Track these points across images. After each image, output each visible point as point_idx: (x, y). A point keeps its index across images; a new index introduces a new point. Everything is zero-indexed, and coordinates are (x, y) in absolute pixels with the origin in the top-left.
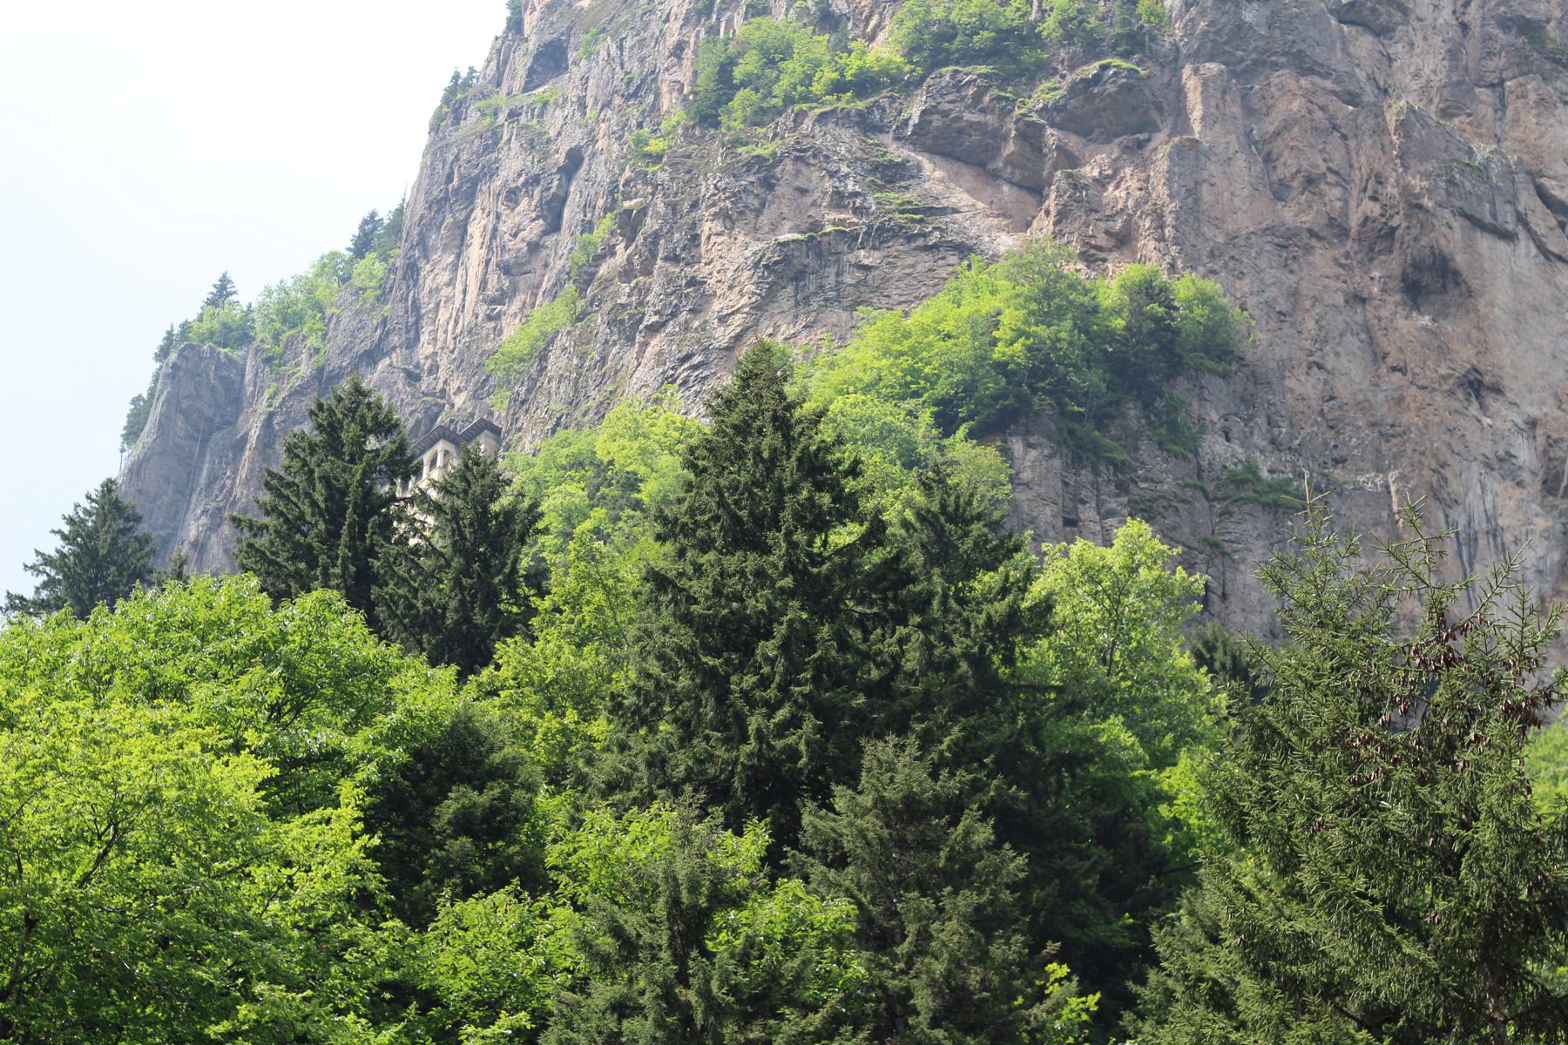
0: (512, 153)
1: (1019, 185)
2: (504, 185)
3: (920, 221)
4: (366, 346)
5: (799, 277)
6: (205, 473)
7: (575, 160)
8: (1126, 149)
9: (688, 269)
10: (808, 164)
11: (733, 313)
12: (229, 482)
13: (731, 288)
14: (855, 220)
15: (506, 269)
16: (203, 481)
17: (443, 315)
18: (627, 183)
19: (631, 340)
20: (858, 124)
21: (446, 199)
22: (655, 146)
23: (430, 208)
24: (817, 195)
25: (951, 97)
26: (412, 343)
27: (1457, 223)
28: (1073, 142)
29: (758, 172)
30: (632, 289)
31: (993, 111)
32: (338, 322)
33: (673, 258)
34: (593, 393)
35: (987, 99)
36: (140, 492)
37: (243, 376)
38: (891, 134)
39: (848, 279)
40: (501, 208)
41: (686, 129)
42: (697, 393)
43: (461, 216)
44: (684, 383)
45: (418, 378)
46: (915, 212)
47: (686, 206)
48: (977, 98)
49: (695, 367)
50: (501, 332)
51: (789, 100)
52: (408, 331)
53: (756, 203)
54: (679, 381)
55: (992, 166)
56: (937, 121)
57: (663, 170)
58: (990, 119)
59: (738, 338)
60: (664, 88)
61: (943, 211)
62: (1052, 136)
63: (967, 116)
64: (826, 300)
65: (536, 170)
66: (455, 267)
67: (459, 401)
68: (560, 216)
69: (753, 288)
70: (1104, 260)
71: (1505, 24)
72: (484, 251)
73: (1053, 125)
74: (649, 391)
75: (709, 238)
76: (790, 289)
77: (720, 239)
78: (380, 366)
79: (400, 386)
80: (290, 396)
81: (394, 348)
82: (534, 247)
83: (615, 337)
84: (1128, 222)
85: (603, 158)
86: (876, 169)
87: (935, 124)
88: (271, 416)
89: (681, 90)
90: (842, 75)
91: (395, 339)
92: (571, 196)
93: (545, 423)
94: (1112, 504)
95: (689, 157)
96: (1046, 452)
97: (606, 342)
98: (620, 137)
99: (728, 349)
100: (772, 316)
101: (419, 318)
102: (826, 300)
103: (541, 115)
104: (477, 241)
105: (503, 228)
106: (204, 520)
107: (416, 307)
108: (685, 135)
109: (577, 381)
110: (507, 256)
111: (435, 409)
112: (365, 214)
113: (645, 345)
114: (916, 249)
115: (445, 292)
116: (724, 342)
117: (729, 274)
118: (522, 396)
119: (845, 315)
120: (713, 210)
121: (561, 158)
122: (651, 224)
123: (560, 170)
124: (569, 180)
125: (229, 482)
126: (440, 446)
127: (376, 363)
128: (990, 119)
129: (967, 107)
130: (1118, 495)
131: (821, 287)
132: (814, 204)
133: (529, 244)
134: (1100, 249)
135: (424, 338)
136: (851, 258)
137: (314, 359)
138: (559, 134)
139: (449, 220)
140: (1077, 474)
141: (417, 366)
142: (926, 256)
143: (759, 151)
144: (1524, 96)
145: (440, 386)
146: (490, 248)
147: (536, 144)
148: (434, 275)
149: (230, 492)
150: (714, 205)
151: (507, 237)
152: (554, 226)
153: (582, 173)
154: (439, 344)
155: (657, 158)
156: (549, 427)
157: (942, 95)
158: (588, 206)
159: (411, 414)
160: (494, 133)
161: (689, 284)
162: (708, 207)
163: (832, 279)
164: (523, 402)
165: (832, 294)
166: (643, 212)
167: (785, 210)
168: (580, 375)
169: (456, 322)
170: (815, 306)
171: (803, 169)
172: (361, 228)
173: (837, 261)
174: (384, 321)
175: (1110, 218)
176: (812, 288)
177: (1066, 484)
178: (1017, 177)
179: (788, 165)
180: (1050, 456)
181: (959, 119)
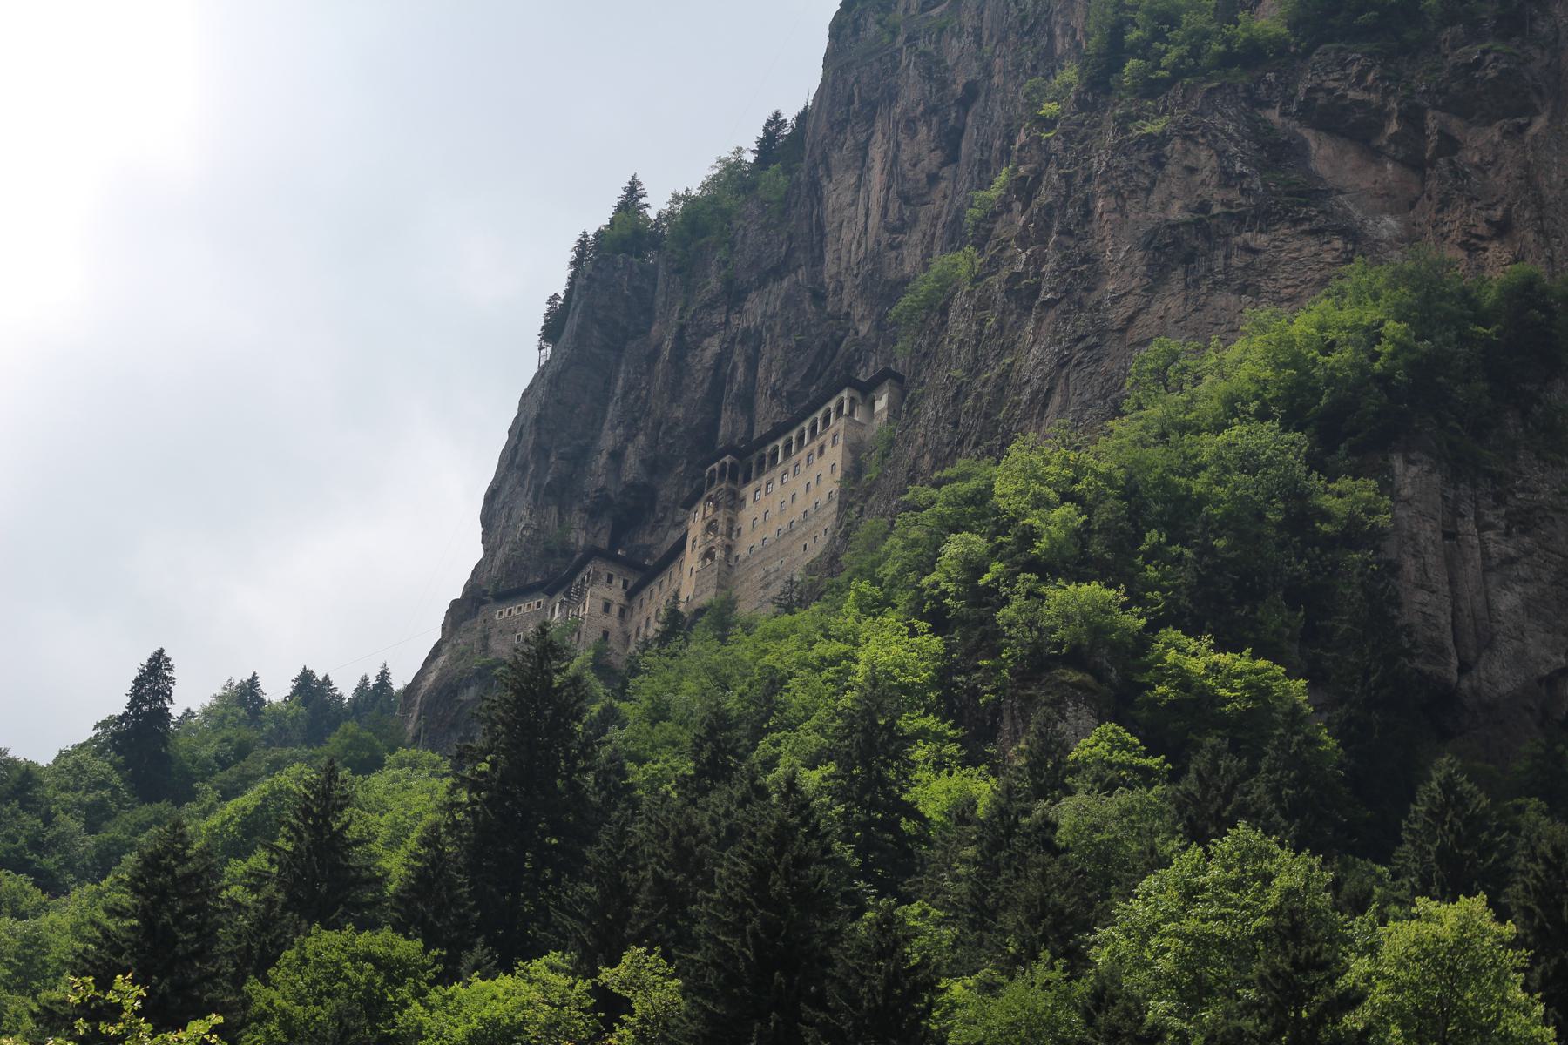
0: (911, 81)
1: (1403, 162)
2: (905, 112)
3: (1306, 205)
5: (1189, 259)
6: (620, 383)
7: (971, 92)
8: (1506, 134)
10: (1197, 143)
12: (644, 392)
13: (1122, 268)
14: (1242, 201)
15: (905, 199)
16: (618, 391)
17: (847, 235)
18: (1022, 148)
19: (1029, 309)
20: (1245, 99)
21: (847, 121)
22: (1049, 109)
23: (832, 128)
24: (1206, 173)
25: (1336, 75)
28: (1455, 125)
29: (1148, 150)
30: (1028, 258)
31: (1376, 90)
32: (745, 235)
35: (1370, 77)
36: (558, 402)
37: (655, 285)
38: (1277, 111)
39: (1236, 262)
40: (901, 136)
41: (1078, 93)
42: (1091, 375)
43: (862, 138)
44: (1079, 363)
45: (823, 298)
46: (1301, 194)
47: (1078, 180)
48: (1361, 77)
49: (1089, 348)
50: (903, 260)
51: (1177, 73)
53: (1147, 183)
54: (1074, 362)
55: (1376, 143)
56: (1321, 99)
57: (1058, 139)
58: (1373, 97)
59: (1131, 319)
60: (1058, 31)
61: (1328, 192)
62: (1432, 121)
63: (1351, 94)
64: (1215, 283)
65: (934, 101)
66: (857, 188)
67: (864, 329)
68: (958, 146)
70: (1485, 250)
72: (884, 176)
73: (1435, 107)
74: (1046, 370)
75: (1102, 214)
76: (1180, 272)
77: (1113, 216)
78: (786, 283)
80: (701, 308)
81: (800, 266)
82: (933, 179)
83: (1013, 306)
84: (1507, 211)
85: (999, 96)
86: (1263, 148)
87: (1319, 102)
88: (682, 328)
89: (1074, 35)
90: (1229, 47)
92: (968, 130)
93: (945, 388)
94: (1490, 517)
95: (1082, 124)
96: (1426, 468)
97: (1003, 312)
98: (1016, 77)
99: (1122, 330)
100: (1163, 298)
101: (823, 236)
102: (1215, 283)
103: (938, 41)
104: (878, 166)
105: (904, 156)
106: (620, 431)
107: (820, 226)
108: (1077, 101)
109: (977, 346)
110: (907, 186)
111: (841, 333)
112: (769, 114)
113: (1040, 320)
114: (1303, 232)
115: (849, 212)
116: (1116, 326)
117: (1122, 255)
118: (924, 349)
119: (1233, 299)
122: (1044, 196)
123: (957, 101)
124: (966, 112)
126: (845, 394)
127: (782, 279)
128: (1373, 97)
129: (1351, 86)
130: (1495, 508)
131: (1210, 270)
132: (1203, 183)
133: (928, 176)
134: (1481, 238)
135: (828, 257)
136: (1238, 239)
137: (722, 273)
138: (956, 64)
139: (850, 142)
140: (1456, 488)
142: (1313, 241)
143: (1149, 129)
145: (845, 309)
146: (890, 175)
147: (933, 70)
148: (838, 191)
150: (1106, 182)
151: (907, 166)
152: (952, 157)
153: (978, 106)
154: (843, 265)
155: (1048, 123)
156: (950, 394)
157: (1327, 73)
158: (985, 146)
159: (819, 335)
160: (893, 57)
161: (1083, 261)
163: (1221, 261)
164: (925, 355)
165: (1221, 277)
166: (1038, 179)
167: (1175, 189)
168: (979, 341)
169: (859, 244)
170: (1204, 289)
171: (1192, 148)
172: (765, 130)
173: (1226, 244)
174: (790, 238)
175: (1490, 206)
176: (1202, 271)
177: (1445, 498)
178: (1401, 155)
179: (1177, 143)
180: (1430, 472)
181: (1343, 96)
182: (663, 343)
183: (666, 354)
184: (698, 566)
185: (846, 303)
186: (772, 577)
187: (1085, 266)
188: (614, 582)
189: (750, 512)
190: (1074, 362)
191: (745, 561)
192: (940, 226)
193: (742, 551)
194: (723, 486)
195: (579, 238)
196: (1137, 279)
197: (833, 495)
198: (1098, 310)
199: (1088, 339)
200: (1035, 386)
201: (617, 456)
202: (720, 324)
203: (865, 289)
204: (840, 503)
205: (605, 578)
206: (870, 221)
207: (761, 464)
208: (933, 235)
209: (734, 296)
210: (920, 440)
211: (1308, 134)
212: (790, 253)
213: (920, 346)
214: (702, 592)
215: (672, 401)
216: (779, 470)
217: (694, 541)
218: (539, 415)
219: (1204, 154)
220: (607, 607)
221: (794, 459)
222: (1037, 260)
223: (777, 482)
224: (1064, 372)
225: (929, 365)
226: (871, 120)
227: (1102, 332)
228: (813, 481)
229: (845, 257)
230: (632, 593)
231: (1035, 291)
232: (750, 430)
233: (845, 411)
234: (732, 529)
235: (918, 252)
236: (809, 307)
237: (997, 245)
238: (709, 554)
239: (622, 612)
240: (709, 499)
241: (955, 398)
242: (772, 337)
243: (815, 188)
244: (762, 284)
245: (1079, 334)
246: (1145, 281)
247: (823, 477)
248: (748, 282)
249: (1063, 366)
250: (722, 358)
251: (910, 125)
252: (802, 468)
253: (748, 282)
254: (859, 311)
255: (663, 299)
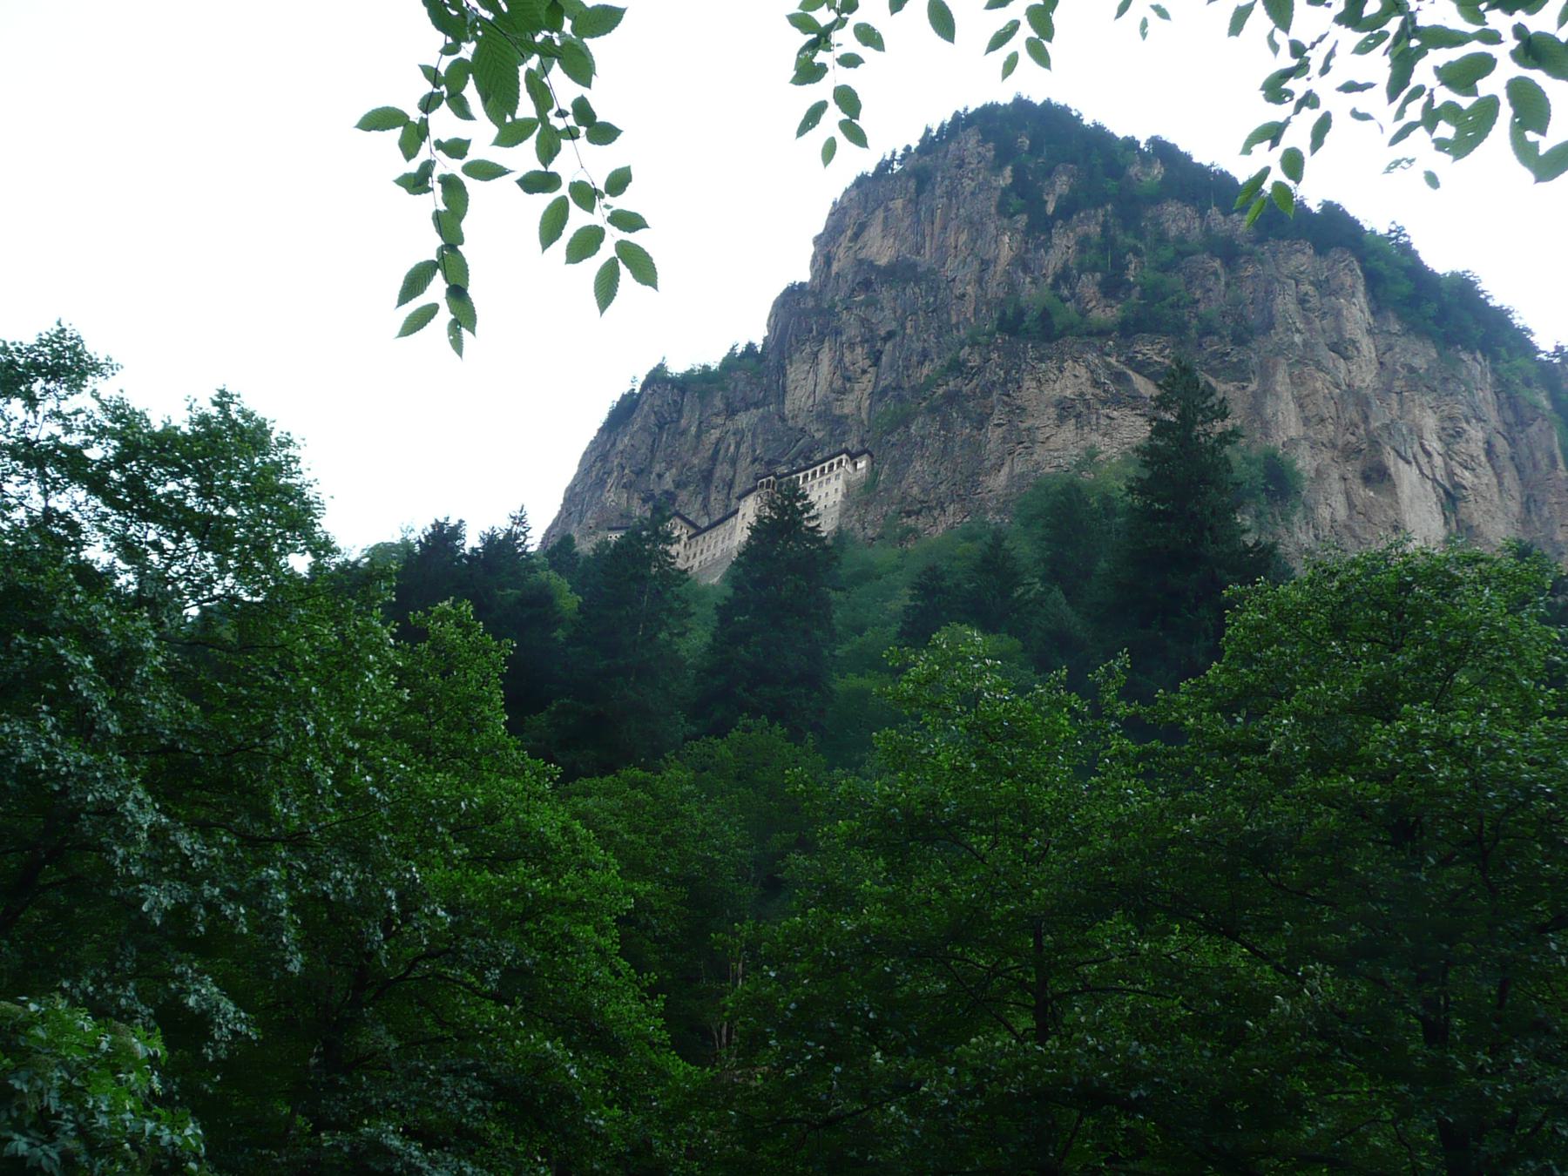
7: (890, 335)
17: (798, 393)
27: (1392, 453)
35: (1167, 351)
48: (1161, 351)
56: (1140, 357)
63: (1155, 358)
65: (867, 336)
71: (1403, 366)
88: (701, 423)
101: (785, 391)
105: (846, 360)
107: (784, 387)
115: (803, 382)
121: (883, 333)
126: (844, 457)
128: (1167, 361)
144: (1413, 401)
148: (796, 373)
152: (876, 362)
206: (818, 388)
209: (731, 412)
210: (911, 480)
211: (1130, 372)
212: (765, 397)
215: (694, 455)
219: (1084, 370)
226: (822, 342)
227: (1033, 442)
230: (690, 538)
232: (734, 476)
236: (779, 425)
243: (781, 370)
244: (747, 409)
250: (719, 440)
251: (852, 346)
252: (816, 488)
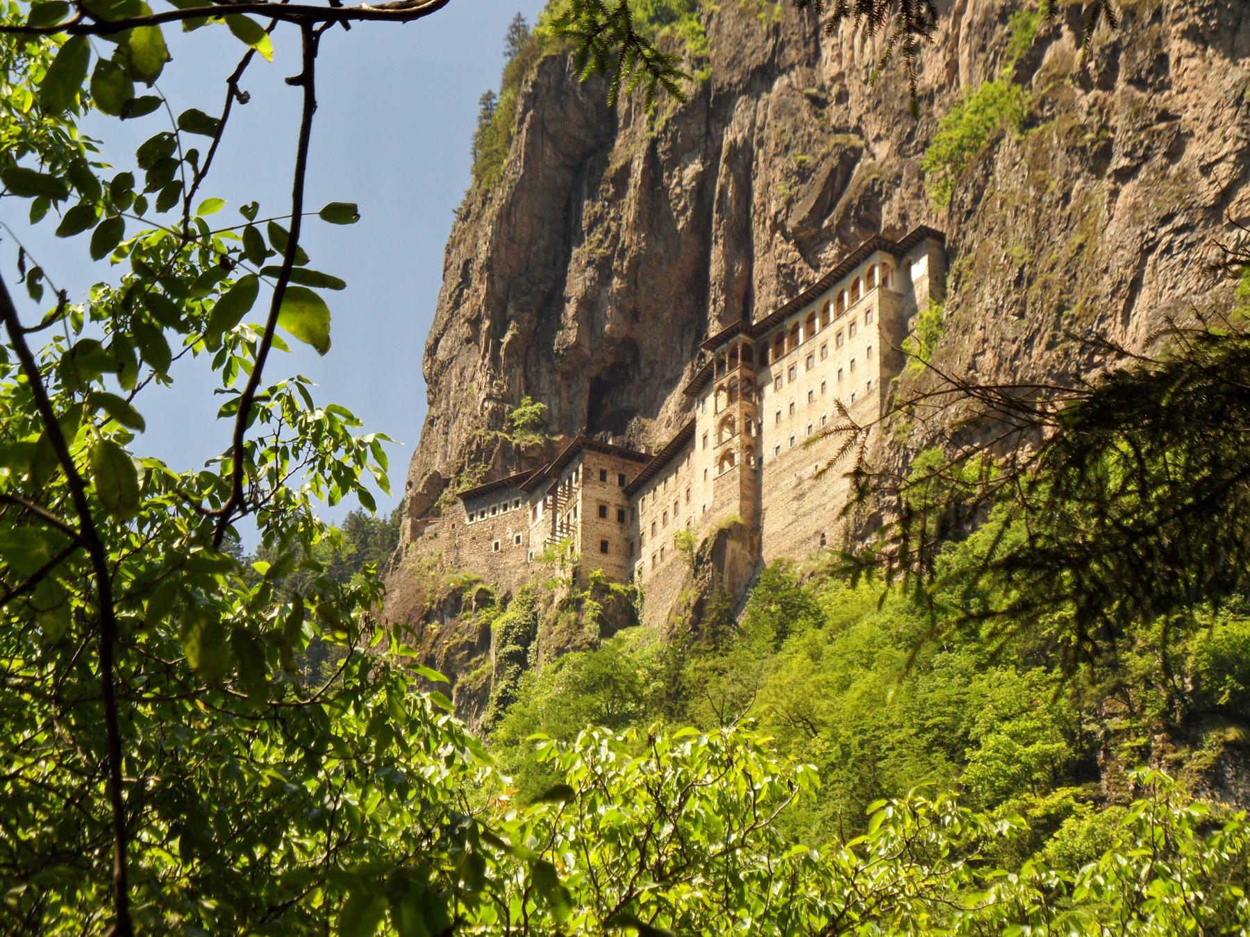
4: (758, 59)
9: (1157, 97)
11: (1218, 162)
13: (1211, 129)
26: (813, 59)
32: (720, 23)
33: (1139, 83)
34: (1059, 239)
42: (1184, 263)
44: (1168, 250)
47: (1147, 16)
49: (1178, 231)
52: (806, 44)
54: (1161, 247)
69: (1237, 130)
74: (1127, 256)
75: (1178, 61)
79: (806, 115)
81: (792, 67)
88: (654, 142)
91: (792, 54)
97: (1067, 174)
99: (1213, 207)
113: (1114, 193)
117: (1208, 111)
118: (968, 205)
120: (1181, 25)
125: (614, 226)
135: (827, 53)
141: (822, 88)
149: (616, 237)
150: (1181, 19)
154: (845, 63)
162: (1175, 22)
164: (969, 213)
182: (631, 161)
183: (636, 176)
184: (714, 471)
185: (854, 114)
186: (806, 485)
187: (1162, 125)
188: (608, 478)
189: (772, 400)
190: (1161, 247)
191: (771, 464)
192: (964, 21)
193: (768, 453)
194: (737, 373)
195: (511, 22)
196: (1230, 142)
197: (873, 386)
198: (1184, 181)
199: (1177, 218)
200: (1117, 278)
201: (589, 304)
202: (700, 136)
203: (879, 102)
204: (883, 396)
205: (597, 475)
207: (779, 342)
208: (957, 36)
212: (779, 49)
213: (962, 201)
214: (723, 505)
216: (802, 352)
217: (705, 438)
218: (489, 259)
220: (603, 512)
221: (819, 339)
222: (1100, 108)
223: (801, 367)
224: (1151, 259)
225: (976, 226)
228: (846, 367)
229: (846, 54)
231: (1106, 153)
233: (877, 281)
234: (753, 418)
235: (941, 55)
237: (1048, 82)
238: (727, 456)
239: (621, 517)
240: (721, 388)
241: (1018, 282)
242: (765, 153)
245: (1165, 213)
246: (1240, 145)
247: (857, 362)
248: (730, 85)
249: (1146, 251)
250: (705, 179)
252: (831, 348)
253: (730, 85)
254: (873, 128)
255: (626, 105)
